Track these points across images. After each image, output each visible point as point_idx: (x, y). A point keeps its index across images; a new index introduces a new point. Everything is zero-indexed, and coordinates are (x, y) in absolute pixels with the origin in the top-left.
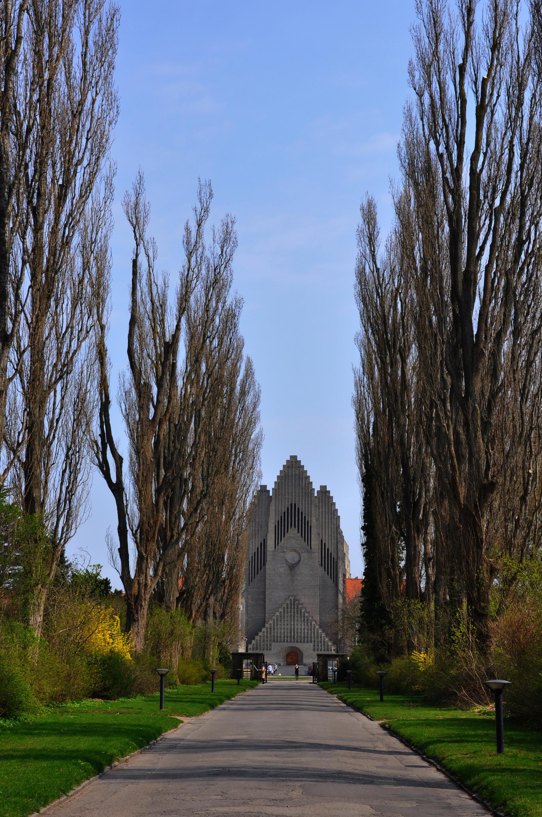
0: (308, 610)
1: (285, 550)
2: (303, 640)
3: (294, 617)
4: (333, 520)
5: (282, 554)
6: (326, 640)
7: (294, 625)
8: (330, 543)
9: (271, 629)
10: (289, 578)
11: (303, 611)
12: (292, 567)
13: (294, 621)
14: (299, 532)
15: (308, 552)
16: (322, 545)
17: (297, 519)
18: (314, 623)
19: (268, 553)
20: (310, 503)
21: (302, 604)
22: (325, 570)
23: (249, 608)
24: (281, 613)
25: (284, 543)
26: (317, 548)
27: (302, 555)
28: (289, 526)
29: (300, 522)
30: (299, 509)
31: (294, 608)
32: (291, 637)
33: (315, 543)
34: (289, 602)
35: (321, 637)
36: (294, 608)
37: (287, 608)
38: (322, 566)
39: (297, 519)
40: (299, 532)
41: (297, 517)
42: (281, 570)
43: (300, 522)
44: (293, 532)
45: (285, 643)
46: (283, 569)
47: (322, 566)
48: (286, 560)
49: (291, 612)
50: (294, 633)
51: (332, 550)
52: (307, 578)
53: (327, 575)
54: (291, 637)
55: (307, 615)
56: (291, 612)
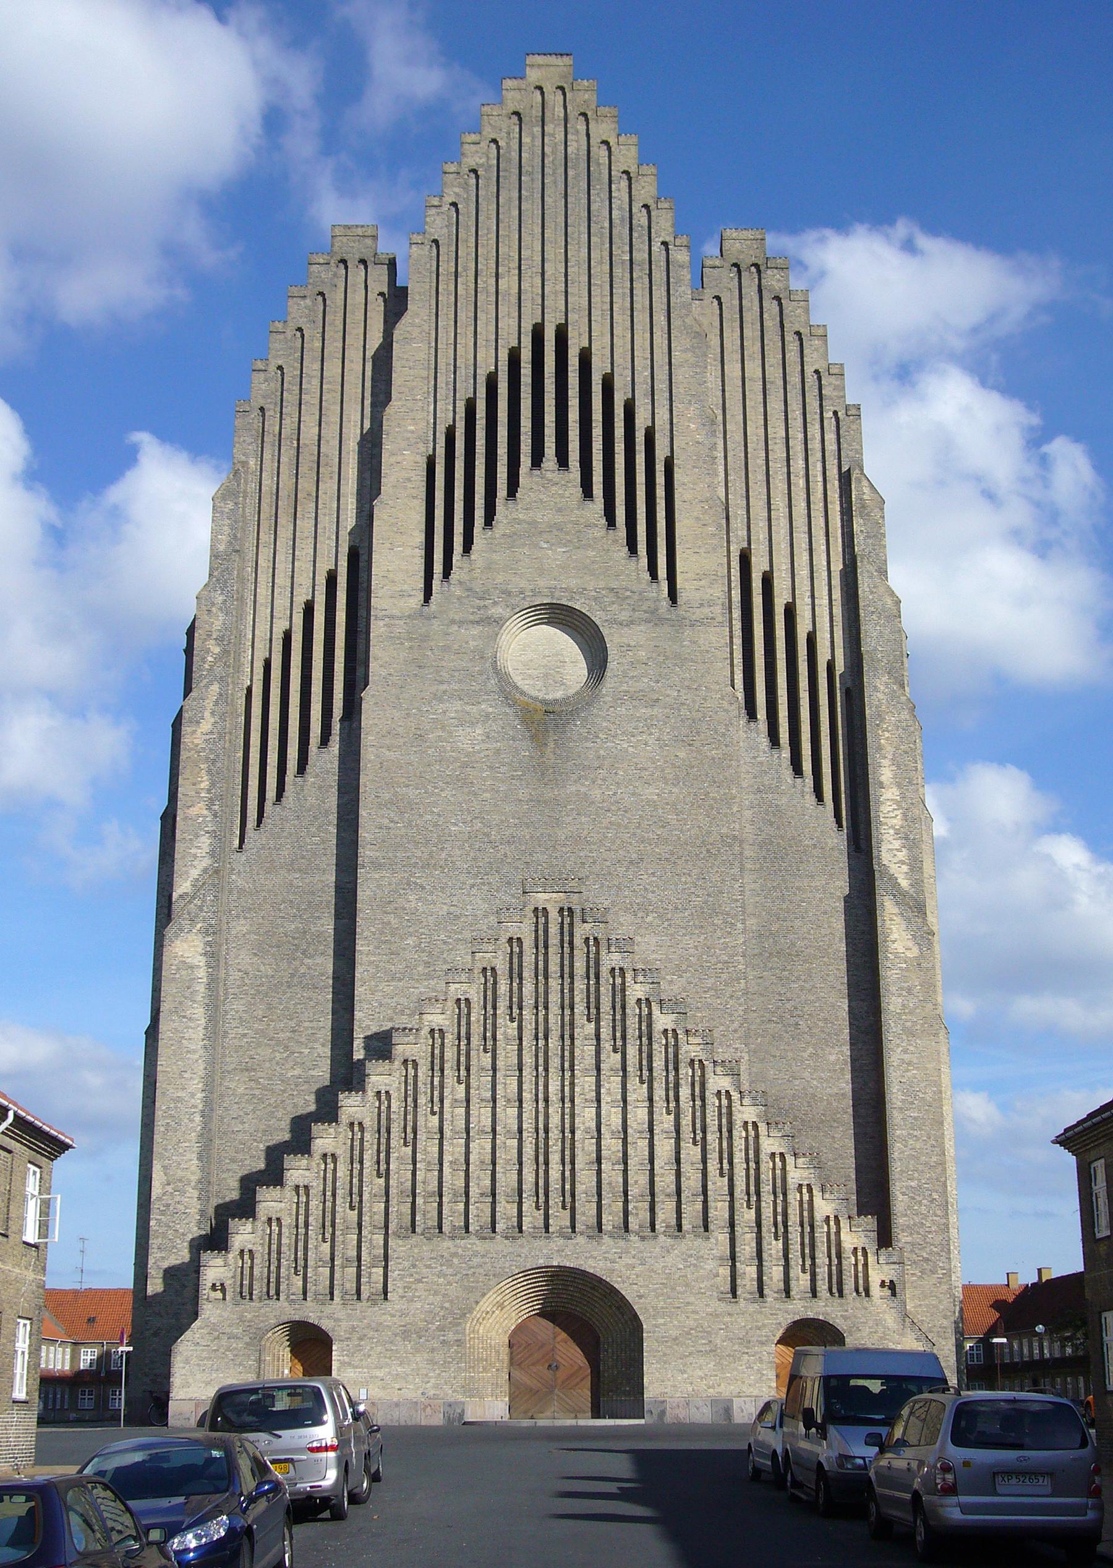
0: (672, 987)
1: (497, 611)
2: (639, 1218)
3: (569, 1035)
4: (814, 430)
5: (472, 635)
6: (824, 1207)
7: (568, 1099)
8: (803, 572)
9: (384, 1130)
10: (523, 793)
11: (636, 991)
12: (545, 722)
13: (569, 1066)
14: (588, 493)
15: (654, 618)
16: (752, 587)
17: (574, 415)
18: (718, 1082)
19: (377, 629)
20: (660, 319)
21: (626, 945)
22: (774, 740)
23: (236, 1007)
24: (463, 1004)
25: (489, 567)
26: (718, 592)
27: (613, 639)
28: (526, 460)
29: (597, 431)
30: (585, 358)
31: (568, 974)
32: (543, 1191)
33: (703, 566)
34: (525, 931)
35: (781, 1189)
36: (568, 974)
37: (516, 974)
38: (752, 714)
39: (574, 415)
40: (588, 493)
41: (574, 403)
42: (470, 738)
43: (597, 431)
44: (549, 495)
45: (500, 1244)
46: (476, 734)
47: (752, 714)
48: (503, 678)
49: (542, 1003)
50: (569, 1160)
51: (819, 616)
52: (650, 792)
53: (787, 772)
54: (543, 1191)
55: (663, 1021)
56: (542, 1003)
